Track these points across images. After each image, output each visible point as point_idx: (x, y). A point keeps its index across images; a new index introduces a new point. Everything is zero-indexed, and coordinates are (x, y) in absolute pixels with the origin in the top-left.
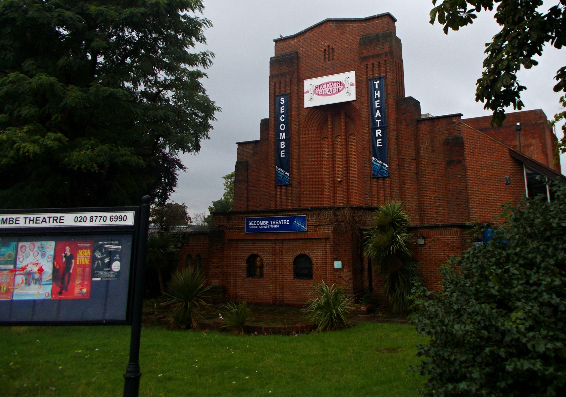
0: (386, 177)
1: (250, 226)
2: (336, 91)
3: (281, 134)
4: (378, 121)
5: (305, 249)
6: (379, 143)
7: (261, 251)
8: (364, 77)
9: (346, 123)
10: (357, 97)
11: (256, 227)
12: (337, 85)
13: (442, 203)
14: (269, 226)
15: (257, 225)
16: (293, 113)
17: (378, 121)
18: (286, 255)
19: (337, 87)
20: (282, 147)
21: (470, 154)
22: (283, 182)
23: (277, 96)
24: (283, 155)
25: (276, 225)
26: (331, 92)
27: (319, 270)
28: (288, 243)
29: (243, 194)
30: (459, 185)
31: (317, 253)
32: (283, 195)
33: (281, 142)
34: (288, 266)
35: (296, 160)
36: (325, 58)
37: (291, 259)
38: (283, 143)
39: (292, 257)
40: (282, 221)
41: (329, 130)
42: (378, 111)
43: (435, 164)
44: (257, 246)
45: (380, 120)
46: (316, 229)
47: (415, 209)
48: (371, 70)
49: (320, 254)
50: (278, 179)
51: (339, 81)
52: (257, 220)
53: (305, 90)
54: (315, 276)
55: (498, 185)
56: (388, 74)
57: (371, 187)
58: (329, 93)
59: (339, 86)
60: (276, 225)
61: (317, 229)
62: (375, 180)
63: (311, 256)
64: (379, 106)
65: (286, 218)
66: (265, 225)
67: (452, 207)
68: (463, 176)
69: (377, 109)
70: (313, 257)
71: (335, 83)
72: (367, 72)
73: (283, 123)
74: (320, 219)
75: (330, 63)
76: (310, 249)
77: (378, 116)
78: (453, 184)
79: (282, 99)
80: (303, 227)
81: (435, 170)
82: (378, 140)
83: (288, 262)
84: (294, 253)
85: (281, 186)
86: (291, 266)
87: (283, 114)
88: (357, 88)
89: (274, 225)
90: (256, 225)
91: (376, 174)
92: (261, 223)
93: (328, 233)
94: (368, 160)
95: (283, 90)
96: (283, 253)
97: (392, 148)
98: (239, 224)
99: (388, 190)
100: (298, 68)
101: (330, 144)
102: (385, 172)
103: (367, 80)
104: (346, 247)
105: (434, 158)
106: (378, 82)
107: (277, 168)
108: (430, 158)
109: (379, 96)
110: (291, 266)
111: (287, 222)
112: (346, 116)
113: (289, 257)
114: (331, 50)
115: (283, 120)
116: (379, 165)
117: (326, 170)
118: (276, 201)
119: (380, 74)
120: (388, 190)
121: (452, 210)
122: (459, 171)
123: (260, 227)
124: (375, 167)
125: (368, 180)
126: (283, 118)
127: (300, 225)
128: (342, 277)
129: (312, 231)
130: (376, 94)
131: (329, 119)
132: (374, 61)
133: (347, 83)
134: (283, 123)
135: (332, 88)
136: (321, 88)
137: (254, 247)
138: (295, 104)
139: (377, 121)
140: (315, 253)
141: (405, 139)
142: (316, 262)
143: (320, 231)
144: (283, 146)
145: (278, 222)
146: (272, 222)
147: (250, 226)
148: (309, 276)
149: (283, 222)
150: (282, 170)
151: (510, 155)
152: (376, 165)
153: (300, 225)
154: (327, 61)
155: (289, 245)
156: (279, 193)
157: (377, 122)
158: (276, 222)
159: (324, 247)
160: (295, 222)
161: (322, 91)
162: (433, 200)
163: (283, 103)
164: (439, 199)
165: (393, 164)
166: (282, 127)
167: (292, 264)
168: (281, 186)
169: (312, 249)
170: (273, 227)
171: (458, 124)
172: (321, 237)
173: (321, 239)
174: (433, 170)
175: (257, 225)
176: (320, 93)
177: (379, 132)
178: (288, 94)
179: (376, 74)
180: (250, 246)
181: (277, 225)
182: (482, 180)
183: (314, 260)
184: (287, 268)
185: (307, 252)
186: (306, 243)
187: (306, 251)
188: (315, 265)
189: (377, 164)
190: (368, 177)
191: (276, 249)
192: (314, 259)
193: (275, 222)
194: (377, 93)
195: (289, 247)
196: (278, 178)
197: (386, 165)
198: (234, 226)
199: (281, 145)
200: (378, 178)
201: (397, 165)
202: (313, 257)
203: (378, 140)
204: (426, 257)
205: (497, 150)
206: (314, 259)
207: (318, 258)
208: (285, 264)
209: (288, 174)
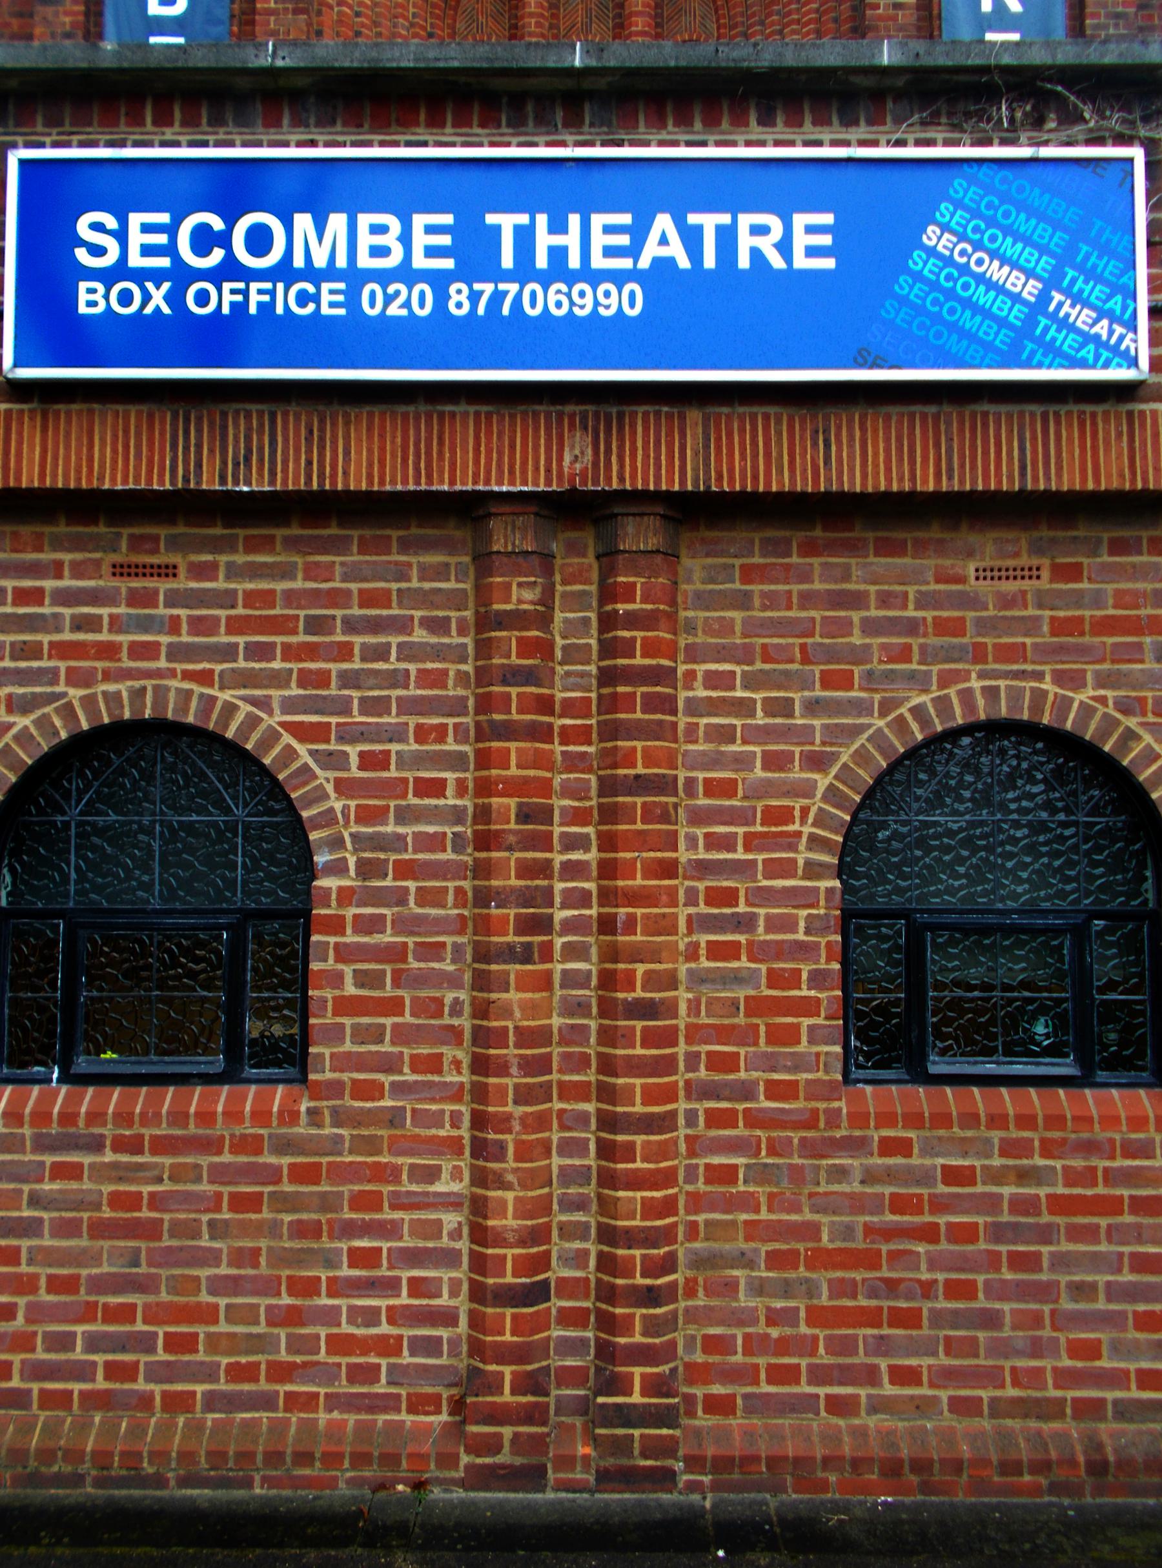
1: (108, 277)
5: (1047, 653)
11: (226, 297)
14: (458, 297)
15: (230, 270)
18: (726, 733)
25: (596, 278)
28: (748, 574)
37: (807, 790)
39: (817, 762)
40: (709, 222)
66: (384, 277)
80: (1082, 317)
83: (750, 843)
84: (861, 708)
86: (805, 898)
90: (217, 276)
96: (668, 705)
110: (805, 898)
111: (801, 241)
113: (773, 761)
123: (286, 299)
137: (145, 624)
145: (639, 232)
146: (525, 237)
147: (108, 277)
153: (1031, 290)
155: (771, 600)
167: (813, 870)
175: (230, 270)
180: (65, 598)
181: (619, 278)
184: (745, 923)
186: (1074, 572)
187: (1060, 678)
191: (545, 649)
193: (571, 240)
208: (703, 868)
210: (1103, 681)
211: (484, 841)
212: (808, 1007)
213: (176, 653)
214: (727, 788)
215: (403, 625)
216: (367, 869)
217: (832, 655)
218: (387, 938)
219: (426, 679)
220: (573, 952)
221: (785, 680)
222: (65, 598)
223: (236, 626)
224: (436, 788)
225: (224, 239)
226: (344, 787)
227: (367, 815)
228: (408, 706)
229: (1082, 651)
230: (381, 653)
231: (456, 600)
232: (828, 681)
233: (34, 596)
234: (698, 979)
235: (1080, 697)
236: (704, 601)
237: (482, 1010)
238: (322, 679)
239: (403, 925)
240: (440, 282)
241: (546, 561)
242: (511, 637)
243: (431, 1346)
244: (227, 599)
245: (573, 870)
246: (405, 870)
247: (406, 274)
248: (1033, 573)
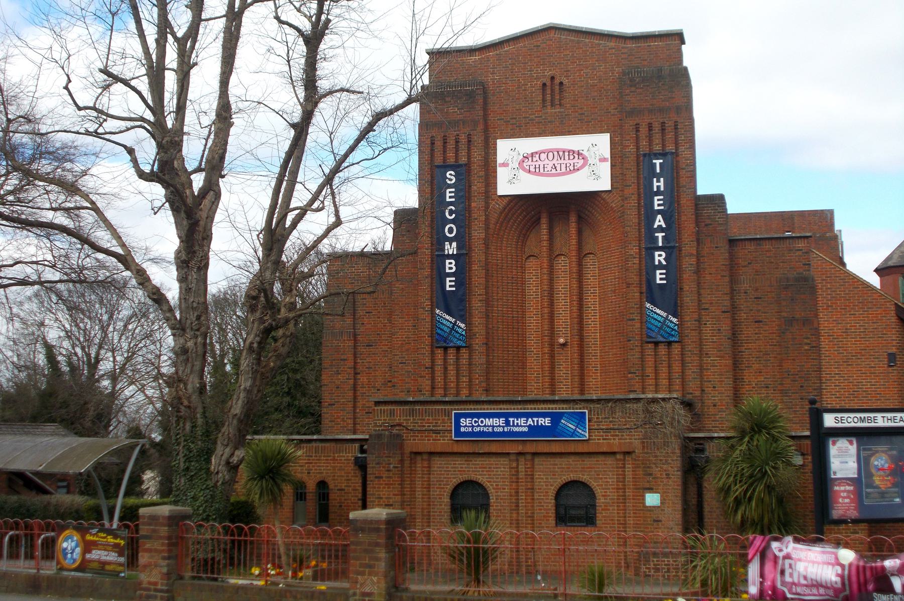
0: (674, 342)
1: (464, 427)
2: (568, 169)
4: (660, 235)
6: (659, 277)
7: (485, 475)
8: (632, 148)
9: (580, 232)
10: (612, 185)
11: (478, 429)
12: (572, 157)
13: (772, 393)
15: (479, 426)
16: (473, 204)
17: (660, 235)
18: (540, 482)
19: (572, 162)
20: (448, 271)
21: (826, 309)
22: (452, 341)
23: (438, 167)
24: (450, 286)
25: (521, 426)
26: (558, 168)
27: (609, 510)
29: (345, 360)
30: (806, 362)
31: (606, 478)
32: (451, 368)
33: (447, 261)
34: (545, 503)
35: (480, 298)
36: (544, 100)
37: (550, 489)
38: (450, 263)
39: (552, 485)
40: (535, 419)
41: (545, 243)
42: (659, 217)
43: (761, 322)
44: (475, 464)
45: (664, 234)
46: (606, 436)
47: (727, 403)
48: (646, 137)
49: (612, 482)
50: (438, 334)
51: (576, 149)
52: (479, 416)
53: (500, 160)
54: (601, 520)
55: (875, 367)
56: (681, 149)
57: (642, 359)
58: (554, 171)
59: (576, 160)
60: (521, 426)
61: (607, 436)
62: (650, 346)
63: (593, 484)
64: (662, 208)
65: (544, 415)
66: (496, 426)
67: (791, 402)
68: (813, 347)
69: (659, 212)
70: (598, 485)
71: (566, 154)
72: (637, 138)
73: (452, 221)
74: (613, 418)
75: (556, 113)
76: (590, 471)
77: (660, 226)
78: (793, 360)
79: (450, 174)
80: (580, 431)
81: (760, 334)
82: (658, 272)
83: (544, 496)
85: (446, 349)
86: (550, 503)
87: (451, 203)
88: (612, 166)
89: (518, 425)
90: (477, 426)
91: (653, 335)
92: (489, 422)
93: (631, 443)
94: (637, 308)
95: (451, 155)
97: (686, 288)
98: (436, 423)
99: (677, 368)
100: (485, 116)
101: (545, 271)
102: (673, 333)
103: (637, 155)
104: (670, 469)
105: (759, 311)
106: (661, 161)
107: (437, 311)
108: (752, 310)
109: (662, 189)
110: (550, 503)
111: (547, 422)
112: (580, 219)
113: (546, 485)
114: (557, 87)
115: (450, 215)
116: (659, 318)
117: (534, 322)
118: (433, 379)
119: (664, 146)
120: (677, 368)
121: (792, 408)
122: (808, 338)
123: (485, 429)
124: (653, 321)
125: (637, 346)
126: (450, 214)
127: (574, 428)
128: (660, 521)
129: (598, 439)
130: (655, 184)
131: (544, 222)
132: (652, 119)
133: (593, 157)
134: (452, 221)
135: (560, 162)
136: (535, 159)
137: (469, 468)
138: (477, 186)
139: (656, 235)
140: (601, 478)
141: (710, 274)
142: (603, 496)
143: (614, 439)
145: (527, 421)
146: (513, 421)
147: (464, 427)
148: (589, 519)
149: (538, 421)
150: (447, 317)
151: (897, 316)
152: (653, 318)
153: (574, 428)
154: (549, 107)
156: (439, 362)
157: (658, 237)
158: (522, 421)
159: (621, 468)
160: (562, 421)
161: (537, 166)
162: (753, 387)
163: (453, 181)
164: (767, 387)
165: (687, 318)
166: (451, 231)
168: (446, 349)
169: (595, 471)
170: (516, 429)
171: (806, 253)
172: (616, 450)
173: (614, 453)
174: (756, 334)
175: (479, 426)
176: (532, 169)
177: (660, 255)
178: (461, 166)
179: (657, 144)
180: (459, 464)
181: (525, 426)
182: (846, 356)
183: (599, 492)
184: (543, 506)
185: (585, 478)
186: (584, 461)
188: (600, 501)
189: (655, 316)
190: (637, 340)
192: (599, 491)
193: (519, 422)
194: (658, 181)
195: (547, 468)
196: (439, 331)
197: (674, 320)
198: (424, 426)
199: (448, 266)
200: (656, 344)
201: (695, 321)
202: (598, 485)
203: (658, 272)
204: (806, 487)
205: (874, 305)
206: (599, 491)
207: (609, 489)
208: (538, 499)
209: (462, 325)
210: (588, 475)
211: (511, 496)
212: (551, 517)
213: (473, 471)
214: (540, 489)
215: (500, 468)
216: (497, 499)
217: (554, 472)
219: (504, 475)
220: (522, 510)
221: (548, 475)
222: (459, 464)
223: (480, 468)
224: (504, 489)
225: (478, 422)
226: (493, 488)
227: (497, 492)
228: (501, 478)
229: (585, 471)
230: (497, 471)
231: (507, 465)
232: (553, 475)
233: (455, 464)
234: (537, 513)
235: (585, 477)
236: (538, 465)
237: (511, 517)
238: (490, 475)
239: (501, 506)
240: (503, 427)
241: (517, 460)
242: (513, 470)
244: (478, 464)
245: (522, 499)
246: (501, 499)
247: (499, 426)
248: (579, 461)
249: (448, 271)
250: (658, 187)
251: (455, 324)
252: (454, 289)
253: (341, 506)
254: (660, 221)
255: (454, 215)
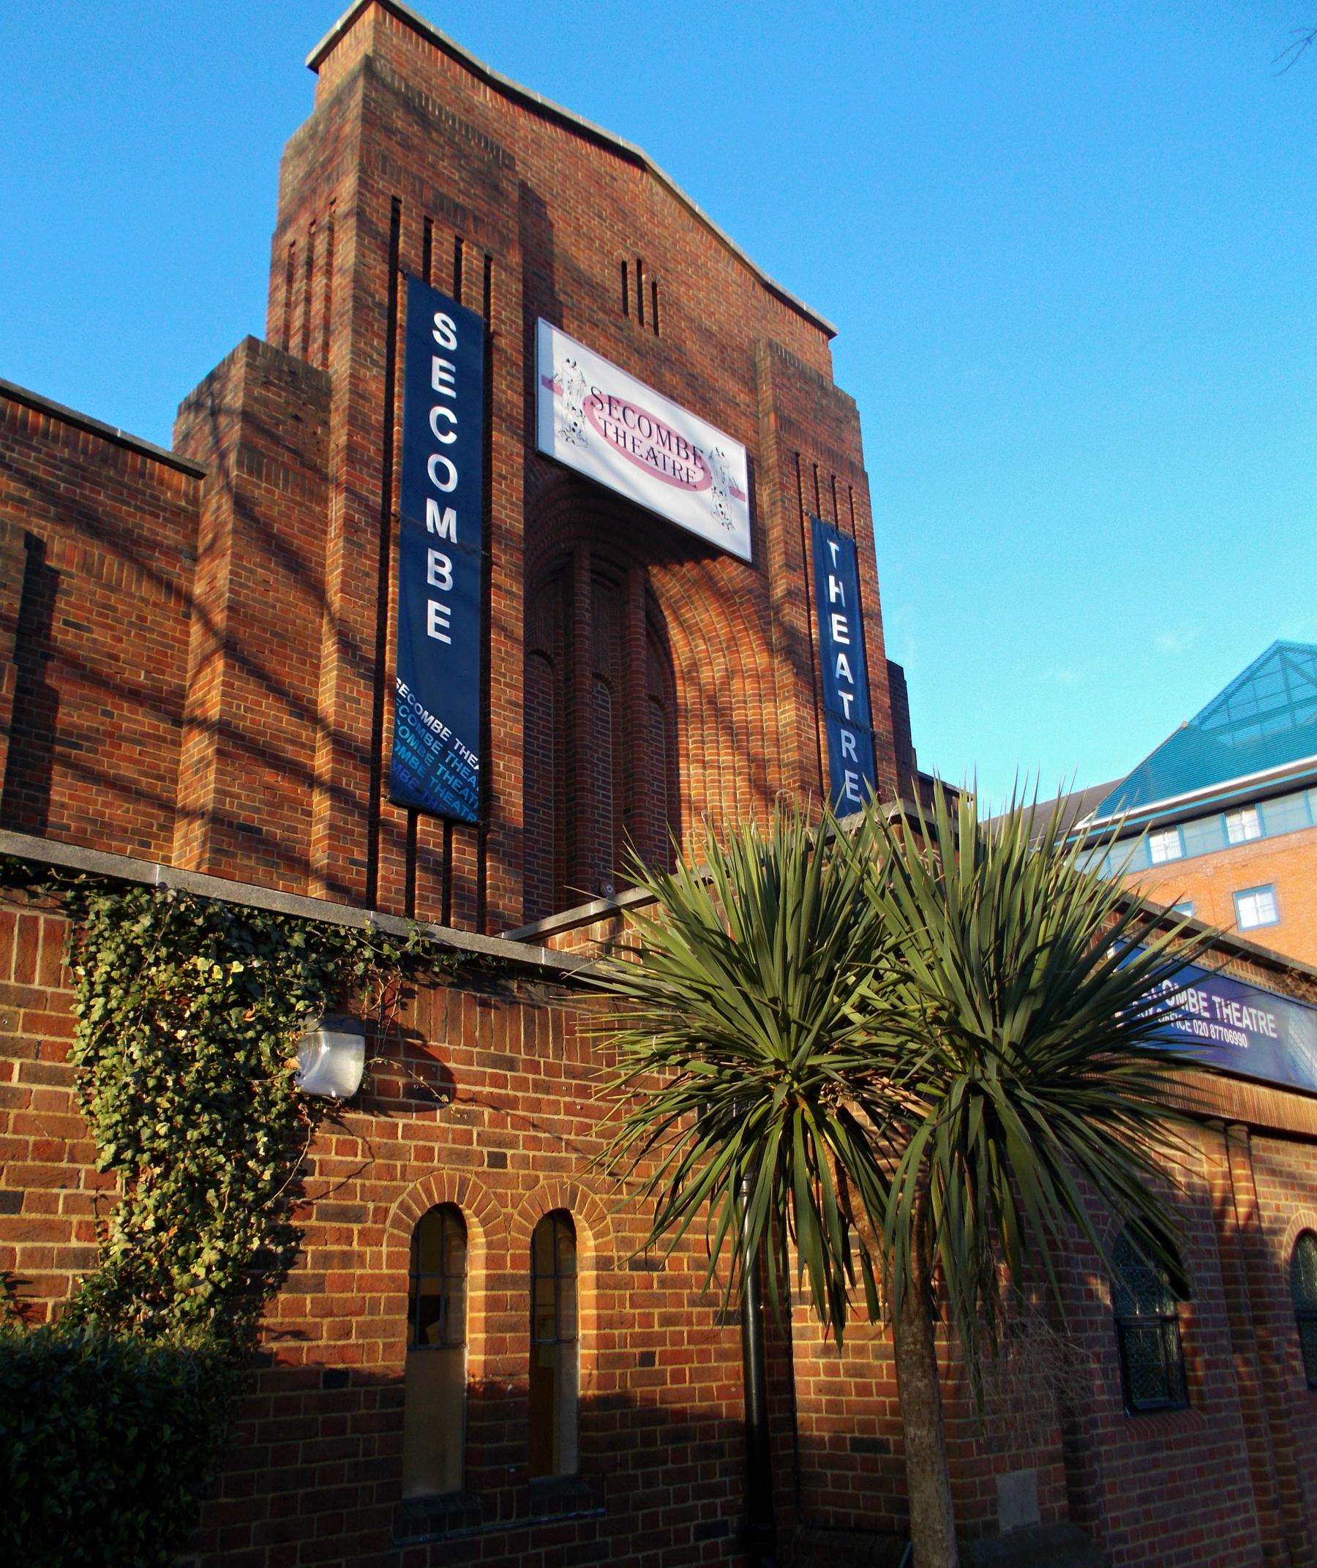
3: (431, 507)
12: (683, 454)
17: (847, 697)
19: (685, 464)
33: (432, 555)
38: (441, 564)
42: (842, 658)
58: (652, 463)
71: (674, 441)
139: (841, 693)
144: (440, 578)
176: (611, 432)
218: (1211, 1329)
243: (1252, 1538)
249: (431, 580)
250: (838, 595)
251: (447, 746)
252: (447, 640)
253: (647, 1359)
254: (842, 668)
255: (450, 438)
